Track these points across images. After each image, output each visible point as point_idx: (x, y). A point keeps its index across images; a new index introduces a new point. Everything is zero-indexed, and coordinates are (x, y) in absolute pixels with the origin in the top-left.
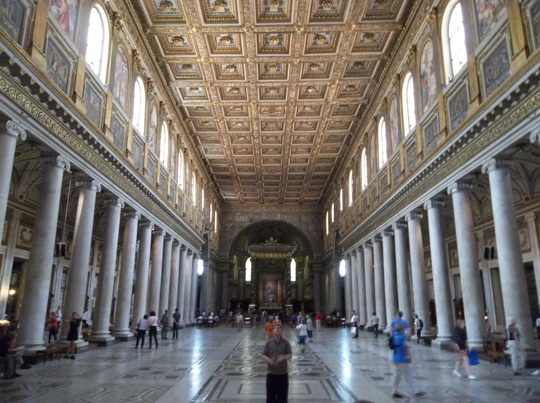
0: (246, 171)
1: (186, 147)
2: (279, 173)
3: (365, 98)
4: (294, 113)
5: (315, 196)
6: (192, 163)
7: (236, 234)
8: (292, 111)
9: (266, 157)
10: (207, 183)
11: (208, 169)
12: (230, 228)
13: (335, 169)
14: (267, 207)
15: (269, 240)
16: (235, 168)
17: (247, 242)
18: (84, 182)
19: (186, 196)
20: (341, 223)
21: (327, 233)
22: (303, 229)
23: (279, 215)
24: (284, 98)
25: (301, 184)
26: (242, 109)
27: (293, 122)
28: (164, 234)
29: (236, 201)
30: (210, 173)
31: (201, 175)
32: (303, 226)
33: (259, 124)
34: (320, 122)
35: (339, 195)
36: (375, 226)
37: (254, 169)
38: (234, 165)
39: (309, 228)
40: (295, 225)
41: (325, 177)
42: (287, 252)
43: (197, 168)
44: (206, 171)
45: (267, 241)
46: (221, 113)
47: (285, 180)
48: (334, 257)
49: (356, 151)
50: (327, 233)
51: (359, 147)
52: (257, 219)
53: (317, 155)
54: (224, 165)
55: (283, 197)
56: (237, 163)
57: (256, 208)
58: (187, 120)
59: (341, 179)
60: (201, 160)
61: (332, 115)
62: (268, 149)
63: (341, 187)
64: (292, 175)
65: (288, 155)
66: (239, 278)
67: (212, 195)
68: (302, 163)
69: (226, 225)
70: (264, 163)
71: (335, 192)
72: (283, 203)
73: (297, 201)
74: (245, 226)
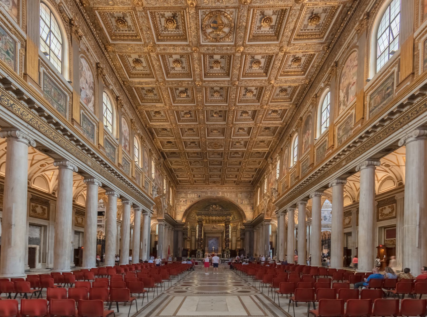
2: (222, 149)
4: (246, 28)
8: (244, 24)
9: (210, 125)
10: (159, 159)
23: (220, 193)
33: (200, 60)
34: (277, 55)
38: (180, 138)
46: (149, 29)
47: (227, 159)
52: (204, 196)
53: (261, 123)
54: (171, 139)
56: (182, 135)
57: (203, 188)
61: (295, 39)
62: (213, 116)
65: (232, 123)
67: (164, 172)
70: (208, 136)
72: (224, 185)
73: (235, 182)
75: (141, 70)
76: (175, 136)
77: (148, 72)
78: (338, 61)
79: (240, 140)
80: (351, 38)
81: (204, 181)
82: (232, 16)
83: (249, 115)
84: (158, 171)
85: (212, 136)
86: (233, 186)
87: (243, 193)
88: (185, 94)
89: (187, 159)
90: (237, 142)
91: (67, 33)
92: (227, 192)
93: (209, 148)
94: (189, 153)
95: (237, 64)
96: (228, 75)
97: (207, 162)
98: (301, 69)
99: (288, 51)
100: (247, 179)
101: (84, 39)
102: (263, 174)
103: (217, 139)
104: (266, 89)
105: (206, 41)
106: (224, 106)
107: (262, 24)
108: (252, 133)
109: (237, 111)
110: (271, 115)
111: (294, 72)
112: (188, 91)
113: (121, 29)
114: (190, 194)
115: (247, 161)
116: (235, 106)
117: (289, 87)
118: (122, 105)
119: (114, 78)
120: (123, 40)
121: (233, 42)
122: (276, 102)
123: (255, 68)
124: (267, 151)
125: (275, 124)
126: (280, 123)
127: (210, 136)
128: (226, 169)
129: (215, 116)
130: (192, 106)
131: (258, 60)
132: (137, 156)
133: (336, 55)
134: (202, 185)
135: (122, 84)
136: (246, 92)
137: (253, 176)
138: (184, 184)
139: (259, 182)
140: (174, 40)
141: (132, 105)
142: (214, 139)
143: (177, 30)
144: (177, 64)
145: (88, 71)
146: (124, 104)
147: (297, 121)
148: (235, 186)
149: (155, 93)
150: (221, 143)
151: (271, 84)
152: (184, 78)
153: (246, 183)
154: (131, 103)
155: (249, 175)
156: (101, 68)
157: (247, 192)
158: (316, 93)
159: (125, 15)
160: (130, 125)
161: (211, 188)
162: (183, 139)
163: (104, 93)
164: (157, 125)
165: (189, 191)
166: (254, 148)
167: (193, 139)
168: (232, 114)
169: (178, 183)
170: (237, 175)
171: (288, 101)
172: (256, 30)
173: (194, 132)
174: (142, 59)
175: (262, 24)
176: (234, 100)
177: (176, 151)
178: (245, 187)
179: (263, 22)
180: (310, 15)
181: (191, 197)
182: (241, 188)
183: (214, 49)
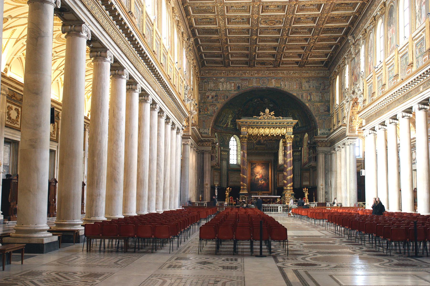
0: (238, 23)
6: (173, 12)
7: (219, 106)
12: (212, 97)
13: (356, 18)
14: (258, 71)
15: (264, 112)
17: (230, 116)
18: (71, 26)
19: (169, 54)
20: (361, 89)
21: (337, 102)
22: (305, 98)
23: (273, 80)
25: (306, 40)
28: (150, 101)
29: (219, 63)
30: (191, 26)
32: (304, 95)
35: (358, 53)
36: (421, 89)
39: (312, 98)
40: (295, 94)
41: (341, 29)
42: (285, 127)
44: (187, 23)
45: (262, 113)
48: (348, 134)
54: (211, 16)
55: (281, 59)
56: (227, 12)
57: (245, 74)
60: (182, 8)
63: (362, 42)
64: (297, 28)
66: (222, 160)
68: (313, 10)
70: (262, 12)
73: (297, 63)
74: (231, 95)
76: (218, 13)
87: (311, 82)
93: (261, 24)
97: (256, 39)
102: (343, 55)
114: (223, 83)
124: (345, 26)
128: (284, 47)
142: (270, 16)
150: (280, 19)
165: (221, 79)
166: (327, 23)
167: (241, 16)
170: (301, 54)
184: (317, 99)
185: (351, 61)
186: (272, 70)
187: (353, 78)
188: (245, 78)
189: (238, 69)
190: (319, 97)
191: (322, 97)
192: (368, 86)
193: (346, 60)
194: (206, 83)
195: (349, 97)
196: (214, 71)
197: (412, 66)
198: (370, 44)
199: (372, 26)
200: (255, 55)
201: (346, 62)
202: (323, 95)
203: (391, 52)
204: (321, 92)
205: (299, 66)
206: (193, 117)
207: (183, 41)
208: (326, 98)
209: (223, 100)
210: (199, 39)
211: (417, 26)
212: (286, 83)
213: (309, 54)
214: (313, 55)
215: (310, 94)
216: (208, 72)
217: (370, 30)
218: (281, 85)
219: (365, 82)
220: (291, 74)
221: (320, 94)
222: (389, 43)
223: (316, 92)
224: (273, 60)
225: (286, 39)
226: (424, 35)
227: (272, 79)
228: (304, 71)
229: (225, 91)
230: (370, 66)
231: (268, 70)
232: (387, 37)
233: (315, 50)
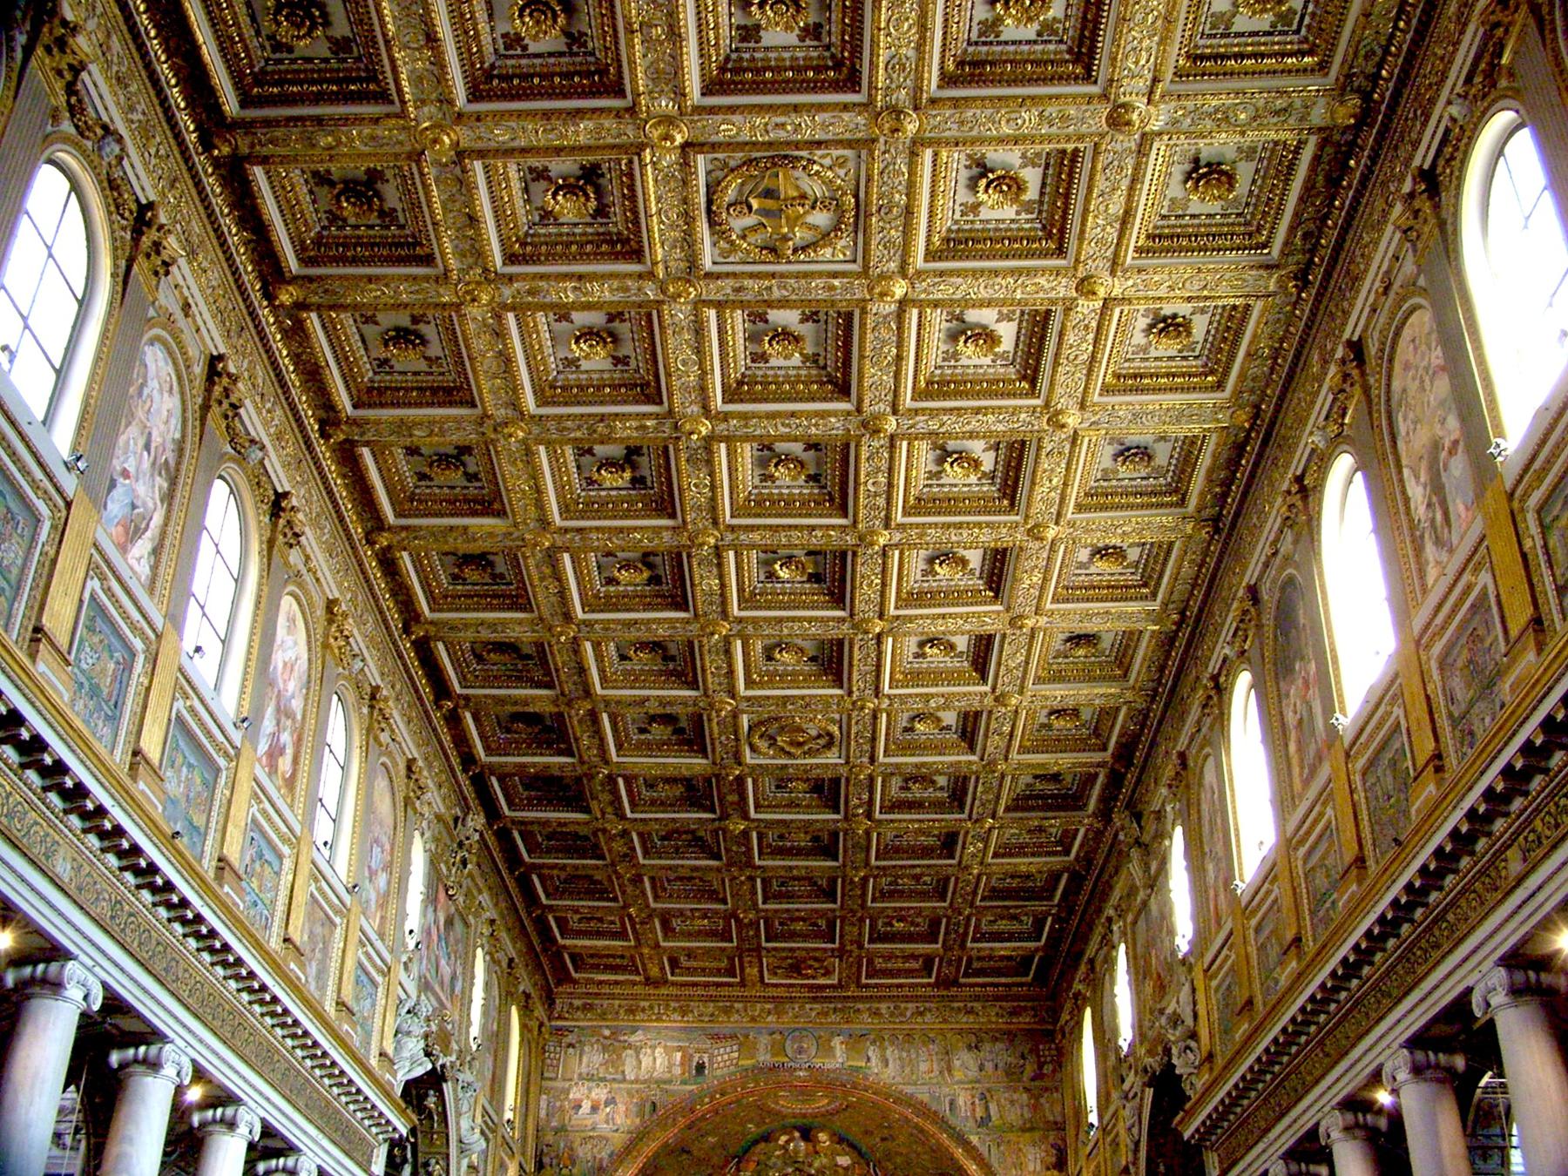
1: (284, 485)
2: (832, 758)
3: (1345, 86)
5: (1019, 936)
6: (330, 622)
9: (755, 621)
10: (456, 819)
11: (453, 720)
12: (595, 1109)
16: (594, 717)
19: (252, 768)
21: (1093, 1118)
23: (836, 1042)
24: (851, 81)
26: (601, 211)
27: (903, 304)
30: (468, 759)
31: (406, 739)
32: (961, 1101)
36: (1515, 866)
37: (698, 721)
38: (587, 693)
43: (376, 680)
44: (447, 739)
49: (1273, 523)
50: (1093, 1118)
51: (1299, 479)
54: (537, 698)
58: (286, 297)
59: (1169, 772)
62: (771, 576)
63: (1170, 816)
67: (485, 898)
69: (574, 1094)
71: (1134, 868)
73: (928, 961)
75: (415, 374)
77: (450, 379)
78: (1360, 338)
79: (932, 704)
80: (1390, 254)
81: (731, 959)
82: (842, 172)
83: (972, 572)
84: (442, 895)
85: (770, 684)
86: (921, 991)
87: (987, 1046)
88: (627, 475)
89: (623, 817)
90: (918, 717)
91: (115, 258)
92: (879, 1040)
93: (753, 749)
94: (636, 777)
95: (884, 343)
96: (843, 390)
97: (745, 834)
98: (1199, 363)
99: (1117, 292)
100: (1003, 948)
101: (183, 271)
102: (1099, 911)
103: (803, 698)
104: (1039, 448)
105: (731, 259)
106: (833, 527)
107: (982, 196)
108: (999, 664)
109: (902, 554)
110: (1092, 570)
111: (1167, 375)
112: (643, 461)
113: (352, 221)
115: (990, 829)
116: (887, 526)
117: (1163, 438)
118: (296, 535)
119: (279, 412)
120: (355, 261)
121: (854, 261)
122: (1104, 508)
123: (972, 357)
124: (1099, 765)
125: (1120, 616)
126: (1149, 613)
127: (761, 685)
128: (865, 880)
129: (784, 574)
130: (657, 530)
131: (984, 327)
132: (331, 801)
133: (1346, 314)
134: (718, 985)
135: (314, 436)
136: (940, 461)
137: (1039, 923)
138: (601, 982)
139: (1083, 968)
140: (582, 256)
141: (346, 530)
143: (600, 220)
144: (591, 346)
145: (166, 395)
146: (307, 530)
147: (1235, 605)
148: (929, 992)
149: (472, 469)
151: (1063, 426)
152: (625, 402)
153: (998, 972)
154: (341, 519)
155: (1014, 917)
156: (229, 375)
157: (1010, 1036)
158: (1298, 473)
159: (374, 176)
160: (320, 631)
161: (779, 1014)
162: (607, 702)
163: (218, 484)
164: (466, 626)
165: (633, 1032)
166: (1023, 750)
167: (663, 702)
168: (878, 570)
169: (563, 977)
171: (1171, 505)
172: (957, 216)
173: (673, 659)
174: (429, 331)
175: (982, 196)
176: (881, 502)
177: (562, 767)
178: (997, 998)
179: (986, 191)
180: (1188, 167)
181: (643, 1075)
182: (970, 1012)
183: (769, 288)
184: (1013, 1116)
185: (1135, 923)
186: (829, 999)
187: (1149, 988)
188: (727, 1031)
189: (701, 991)
190: (1022, 1107)
191: (1035, 1108)
192: (1216, 991)
193: (1115, 928)
194: (571, 1050)
195: (1136, 1073)
196: (606, 1003)
197: (1439, 769)
198: (1205, 807)
199: (1208, 720)
200: (754, 924)
201: (1116, 937)
202: (1037, 1099)
203: (1307, 783)
204: (1027, 1090)
205: (937, 985)
206: (471, 1167)
207: (407, 802)
208: (1048, 1114)
209: (638, 1121)
210: (516, 834)
211: (1432, 573)
212: (888, 1052)
213: (968, 919)
214: (984, 928)
215: (983, 1097)
216: (585, 1005)
217: (1202, 748)
218: (869, 1059)
219: (1201, 976)
220: (908, 1014)
221: (1025, 1096)
222: (1292, 748)
223: (1008, 1088)
224: (833, 950)
225: (868, 833)
226: (1485, 578)
227: (832, 1035)
228: (956, 1005)
229: (645, 1082)
230: (1216, 896)
231: (815, 999)
232: (1283, 725)
233: (991, 898)
